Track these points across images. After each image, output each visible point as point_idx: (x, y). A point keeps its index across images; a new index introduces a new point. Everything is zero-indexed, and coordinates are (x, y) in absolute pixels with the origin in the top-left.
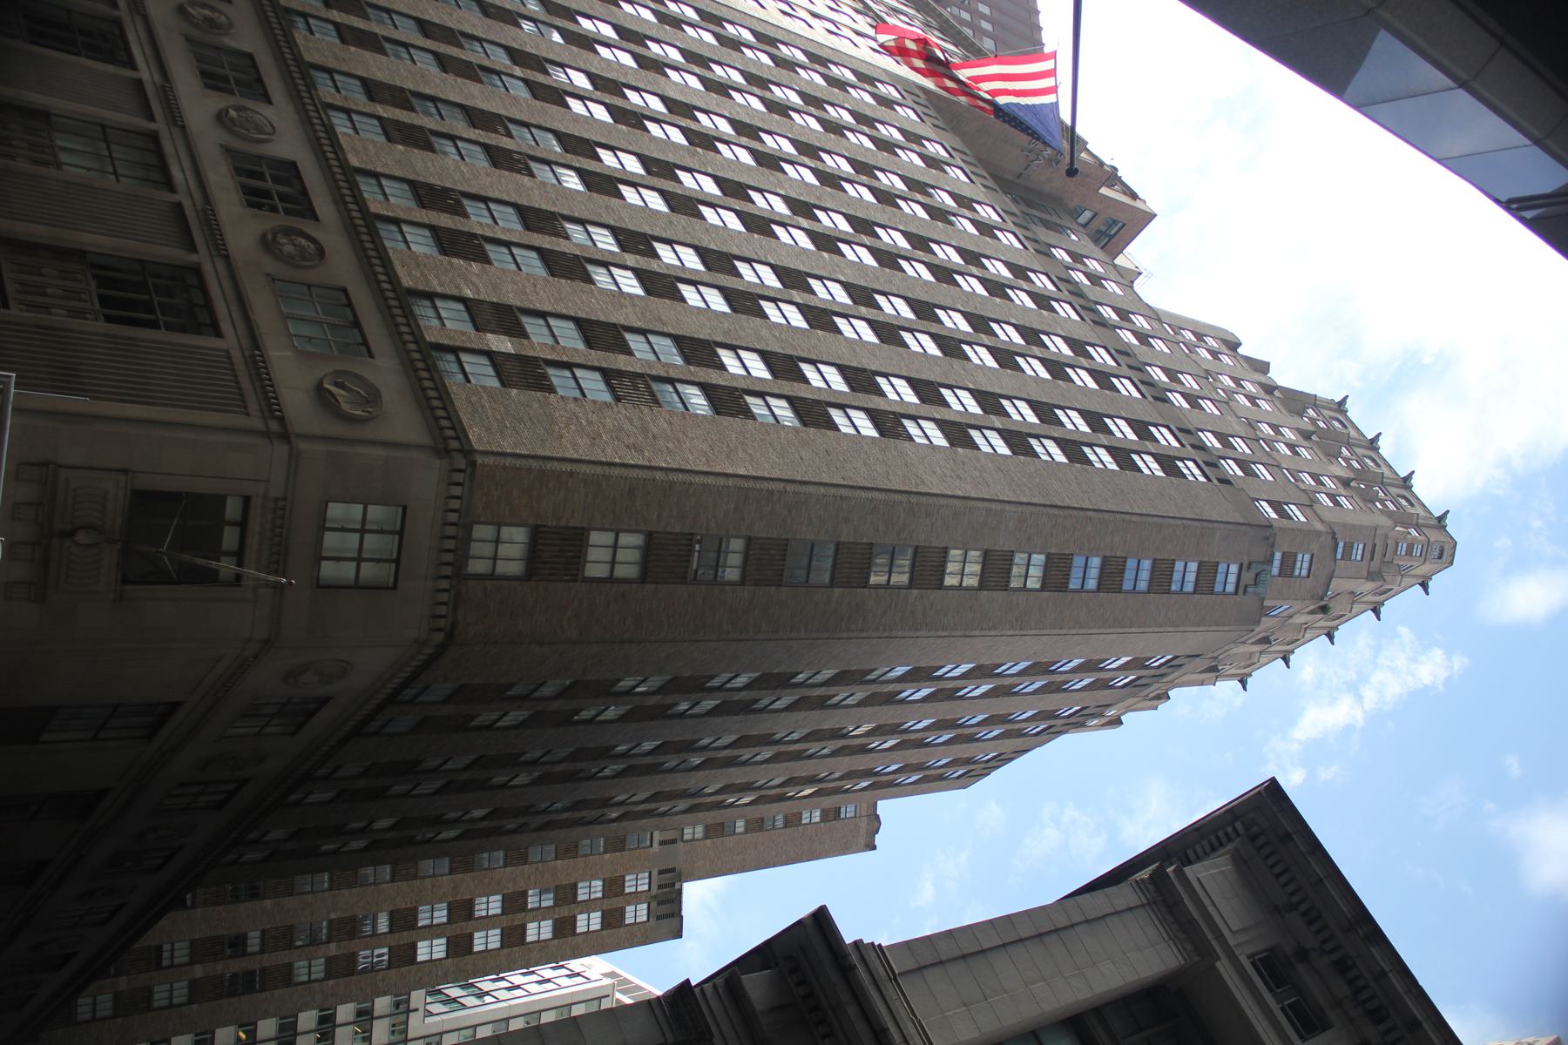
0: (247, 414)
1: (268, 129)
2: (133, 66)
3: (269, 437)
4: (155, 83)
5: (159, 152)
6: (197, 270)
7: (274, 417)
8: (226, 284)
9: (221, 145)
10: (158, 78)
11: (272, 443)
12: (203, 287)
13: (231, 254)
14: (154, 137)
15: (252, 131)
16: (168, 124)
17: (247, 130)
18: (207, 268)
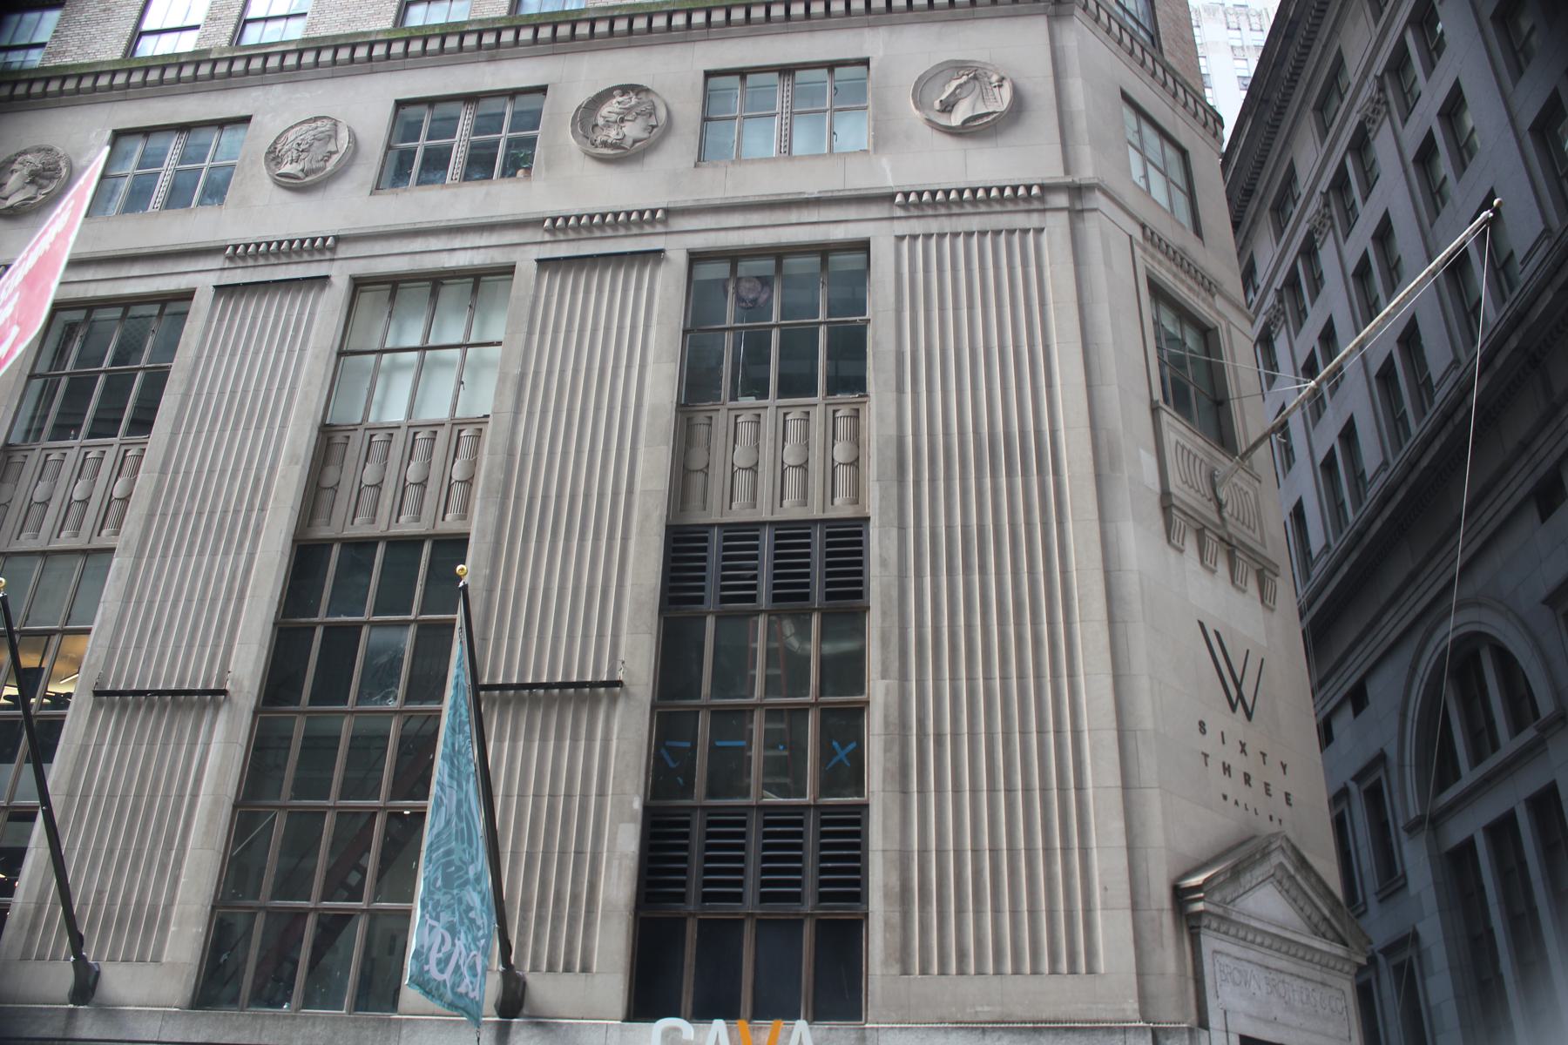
0: (1042, 230)
1: (324, 126)
2: (187, 295)
3: (1082, 211)
4: (223, 269)
5: (394, 284)
6: (696, 258)
7: (1041, 199)
8: (755, 218)
9: (371, 193)
10: (218, 262)
11: (1095, 210)
12: (734, 256)
13: (665, 206)
14: (359, 284)
15: (331, 147)
16: (332, 260)
17: (331, 153)
18: (700, 242)
